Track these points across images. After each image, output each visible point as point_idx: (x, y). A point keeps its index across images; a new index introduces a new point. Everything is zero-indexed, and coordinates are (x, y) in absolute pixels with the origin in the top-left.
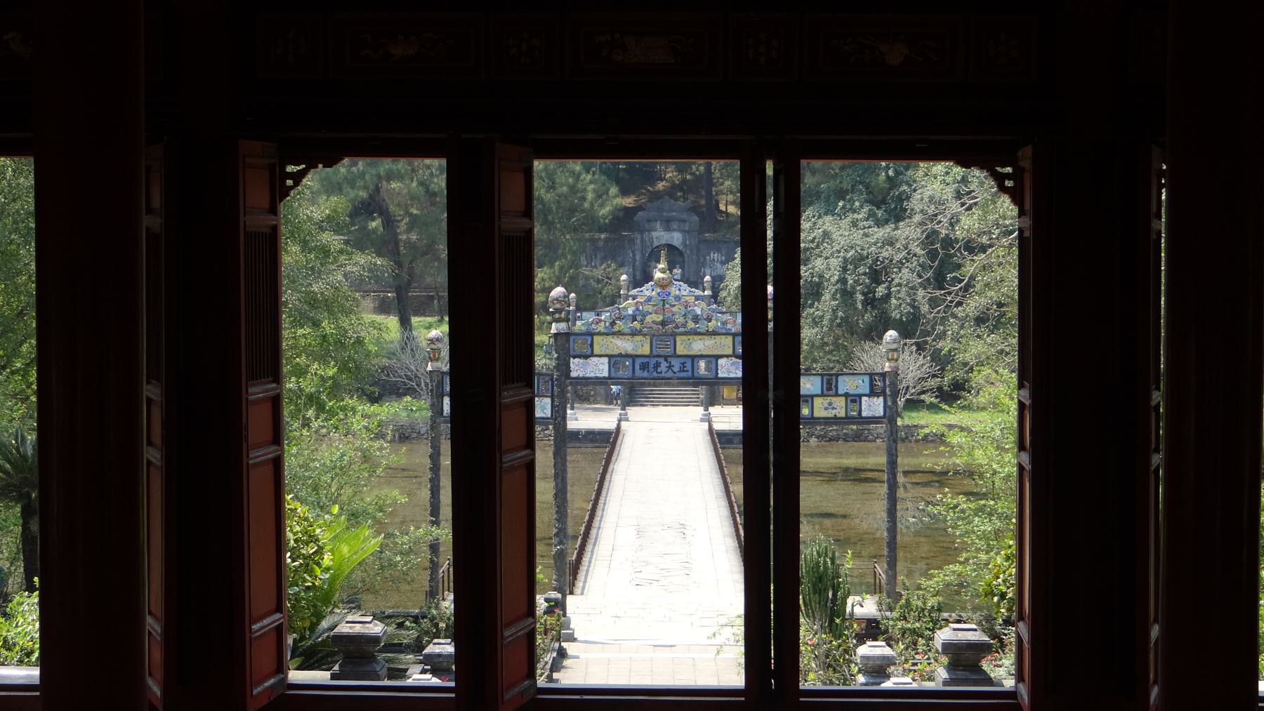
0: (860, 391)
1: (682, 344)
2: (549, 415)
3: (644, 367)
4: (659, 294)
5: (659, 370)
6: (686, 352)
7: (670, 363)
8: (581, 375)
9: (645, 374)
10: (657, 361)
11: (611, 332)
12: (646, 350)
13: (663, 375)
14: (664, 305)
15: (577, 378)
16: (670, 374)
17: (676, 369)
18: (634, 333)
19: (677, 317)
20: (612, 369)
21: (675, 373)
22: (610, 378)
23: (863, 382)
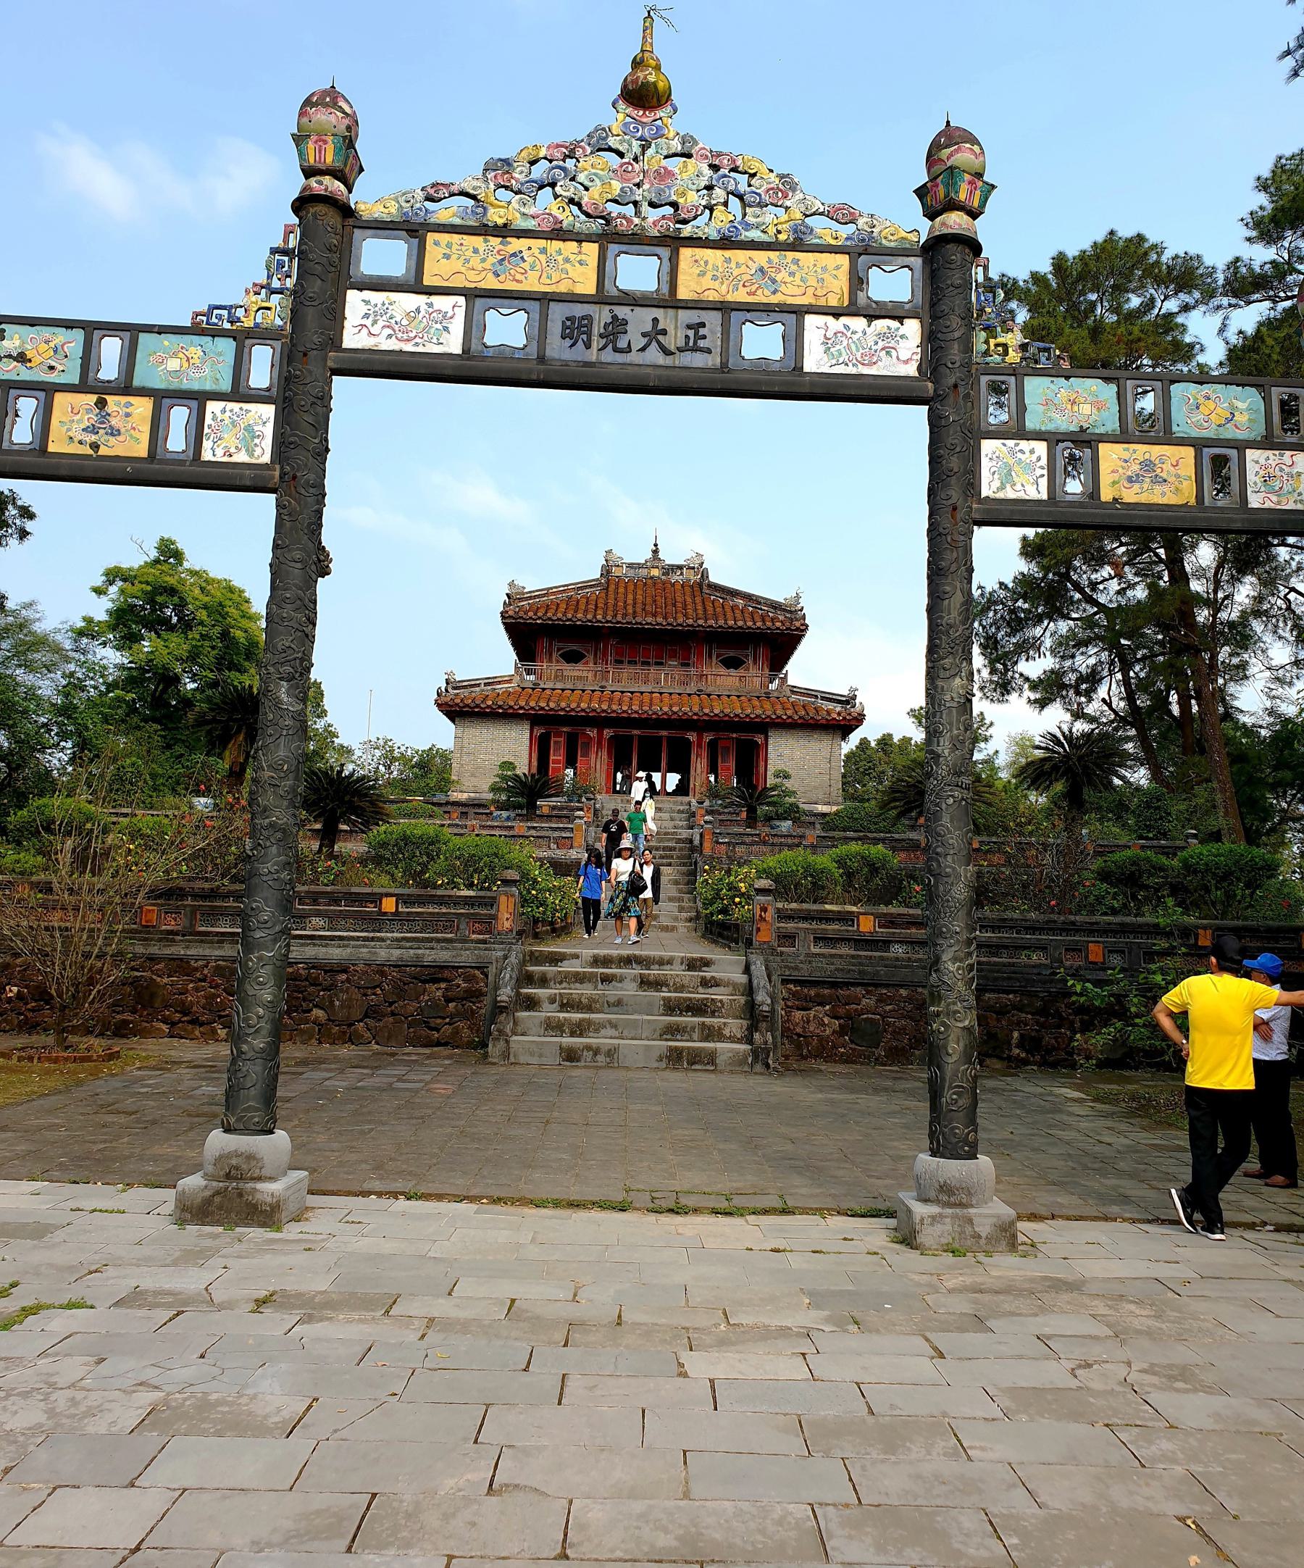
5: (622, 344)
21: (667, 352)
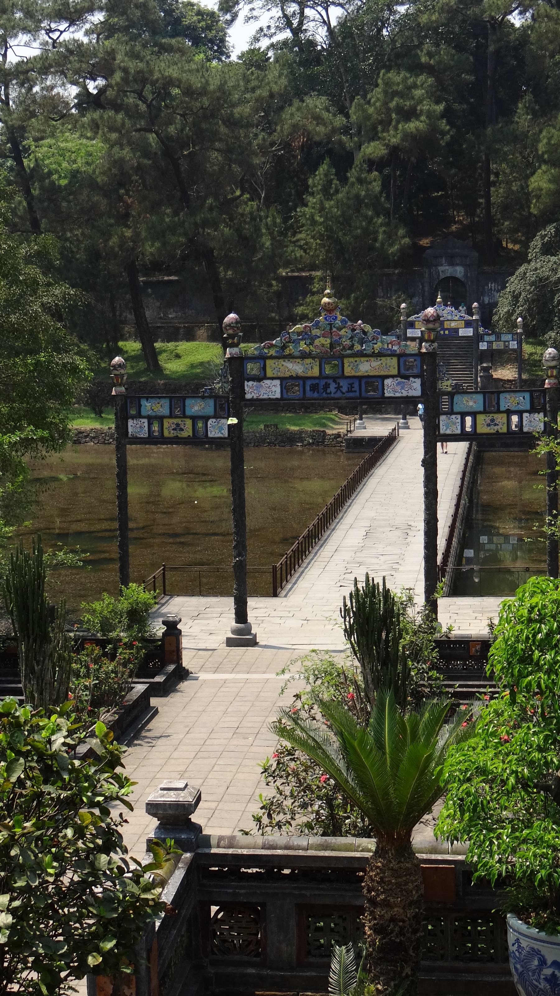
0: (521, 408)
1: (349, 366)
2: (226, 435)
3: (314, 388)
4: (326, 318)
5: (328, 391)
6: (353, 374)
7: (339, 383)
8: (255, 397)
9: (316, 395)
10: (326, 383)
11: (282, 357)
12: (316, 372)
13: (332, 395)
14: (331, 329)
15: (252, 400)
16: (338, 395)
17: (344, 389)
18: (304, 356)
19: (344, 340)
20: (285, 391)
21: (343, 393)
22: (282, 399)
23: (524, 398)
